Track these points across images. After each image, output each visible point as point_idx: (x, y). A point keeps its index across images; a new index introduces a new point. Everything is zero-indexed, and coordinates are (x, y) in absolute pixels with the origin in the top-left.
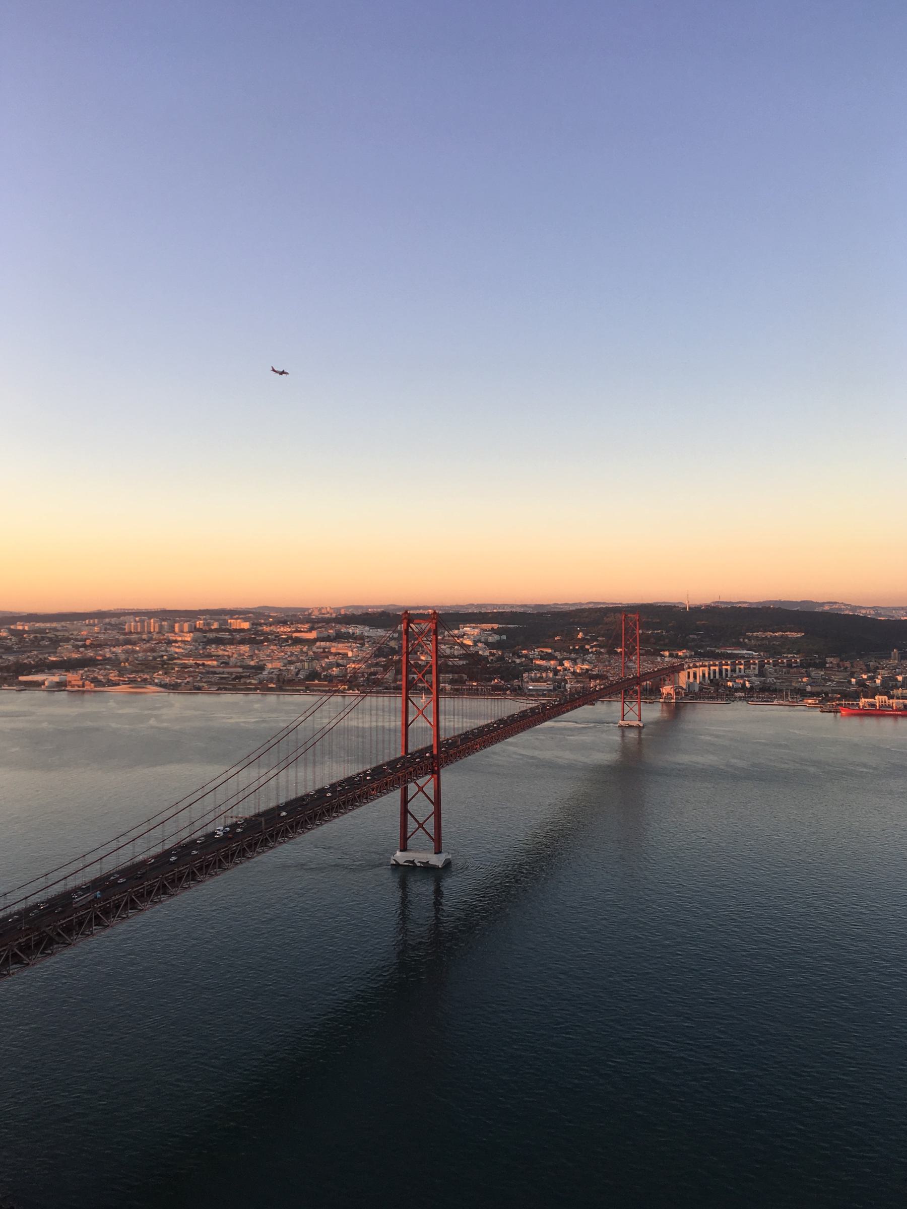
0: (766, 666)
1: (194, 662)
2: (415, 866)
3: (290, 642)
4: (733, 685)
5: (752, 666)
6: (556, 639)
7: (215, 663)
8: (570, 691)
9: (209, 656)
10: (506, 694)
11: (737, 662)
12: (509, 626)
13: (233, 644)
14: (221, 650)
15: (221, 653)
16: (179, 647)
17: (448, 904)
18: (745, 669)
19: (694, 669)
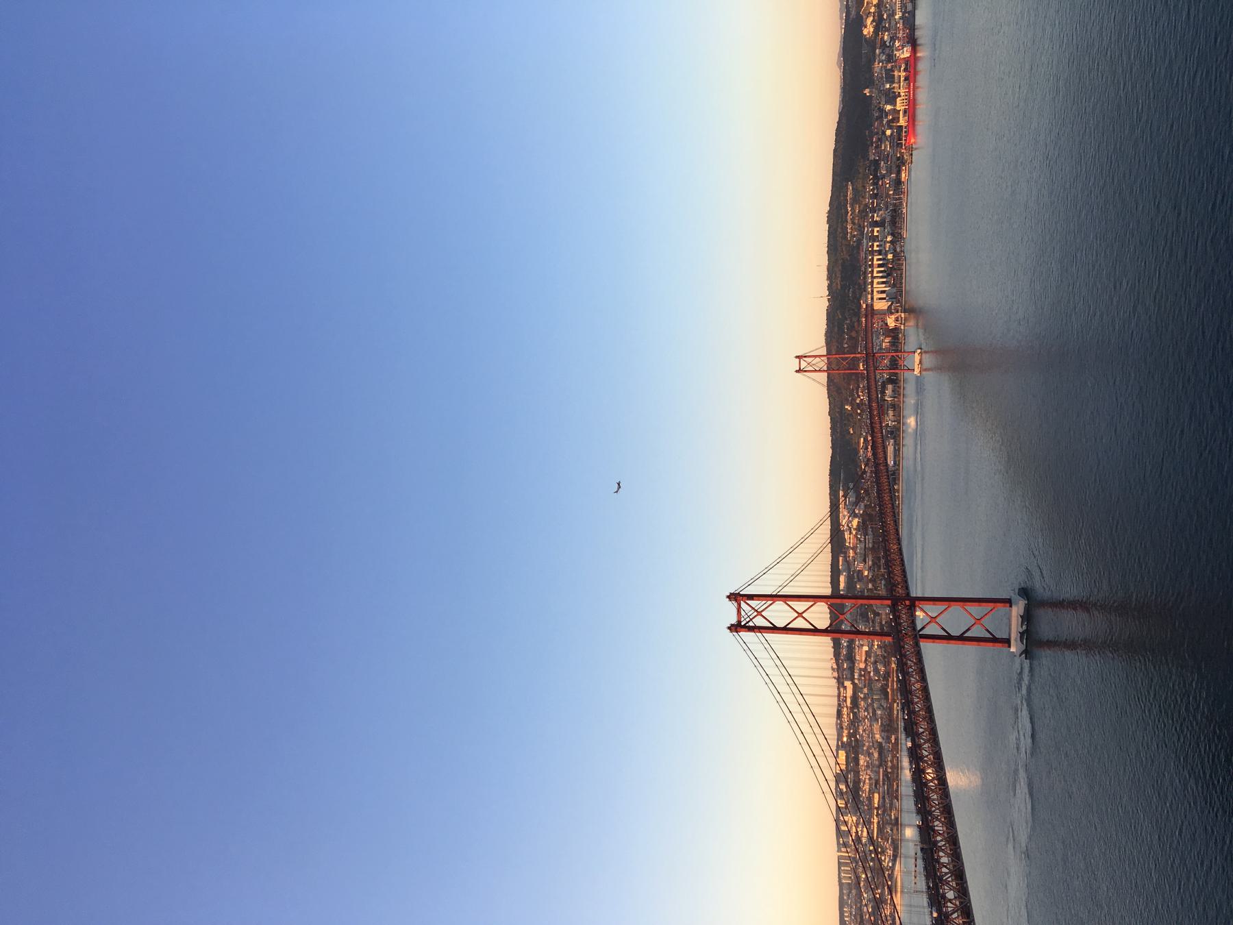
1: (875, 817)
2: (1027, 631)
3: (856, 710)
4: (891, 253)
5: (876, 234)
6: (852, 432)
7: (876, 795)
8: (894, 421)
9: (870, 799)
11: (870, 249)
12: (842, 478)
13: (859, 771)
14: (863, 786)
15: (867, 787)
16: (862, 831)
17: (1070, 591)
18: (878, 241)
19: (875, 293)
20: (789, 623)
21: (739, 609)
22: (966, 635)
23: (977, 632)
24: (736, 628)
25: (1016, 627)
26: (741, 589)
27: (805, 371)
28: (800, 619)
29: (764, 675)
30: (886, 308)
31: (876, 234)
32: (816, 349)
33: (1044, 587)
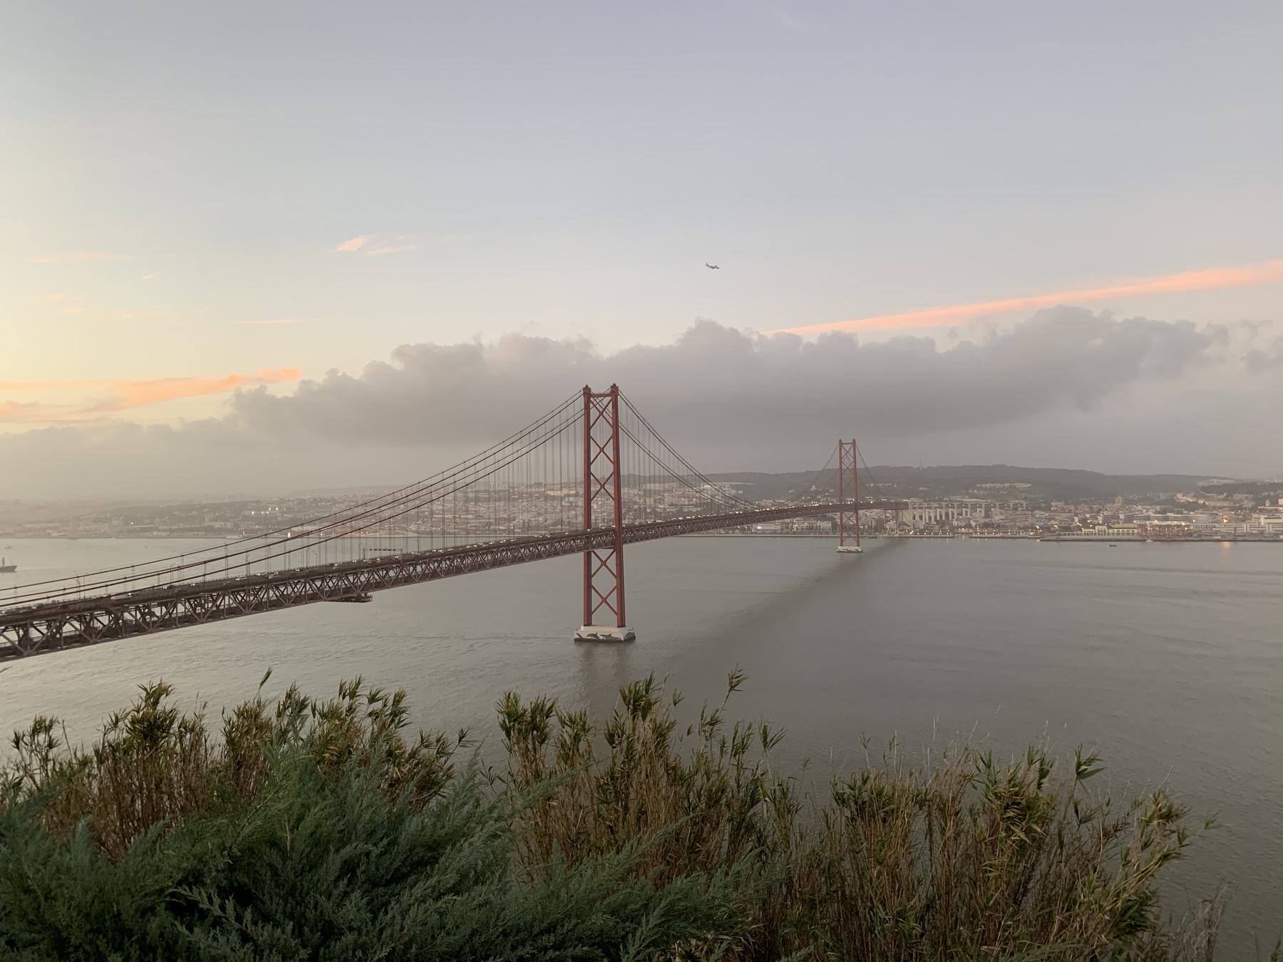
0: (992, 509)
5: (978, 509)
6: (790, 492)
10: (734, 533)
19: (920, 510)
20: (593, 439)
21: (604, 395)
22: (593, 590)
23: (596, 600)
24: (587, 392)
25: (601, 631)
26: (622, 396)
27: (840, 449)
28: (599, 451)
29: (546, 419)
30: (905, 520)
31: (978, 509)
32: (862, 459)
33: (635, 654)
